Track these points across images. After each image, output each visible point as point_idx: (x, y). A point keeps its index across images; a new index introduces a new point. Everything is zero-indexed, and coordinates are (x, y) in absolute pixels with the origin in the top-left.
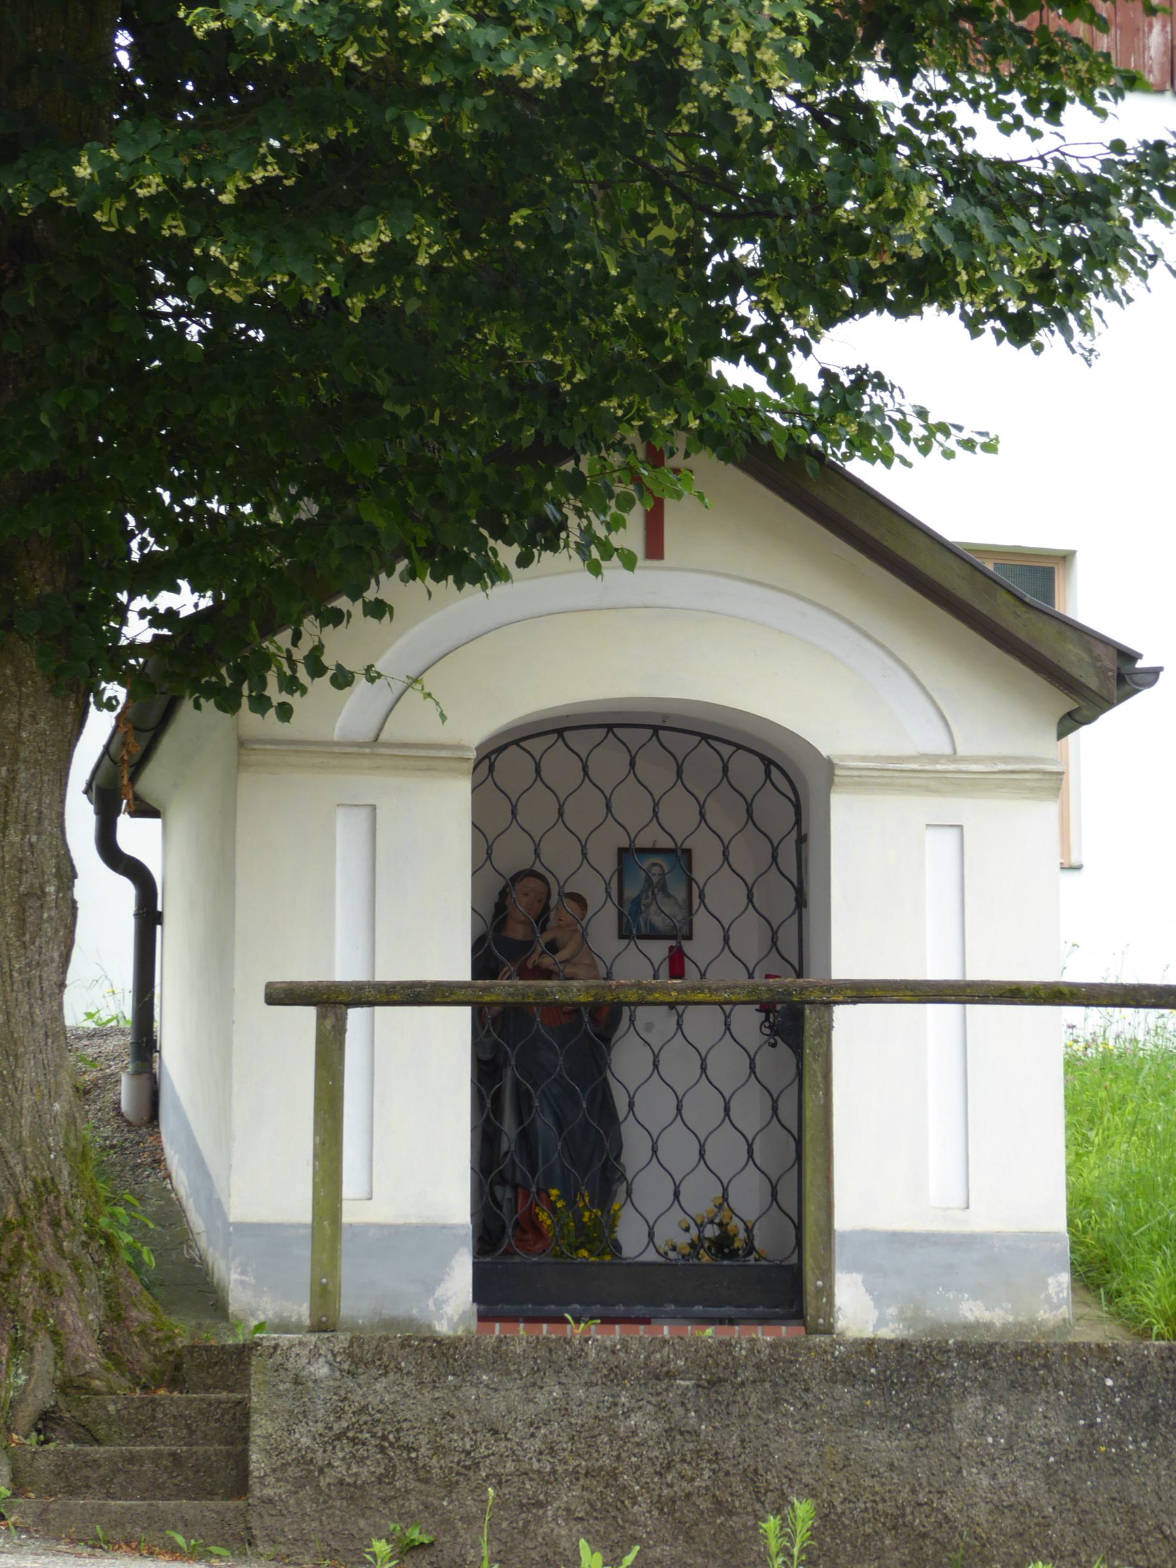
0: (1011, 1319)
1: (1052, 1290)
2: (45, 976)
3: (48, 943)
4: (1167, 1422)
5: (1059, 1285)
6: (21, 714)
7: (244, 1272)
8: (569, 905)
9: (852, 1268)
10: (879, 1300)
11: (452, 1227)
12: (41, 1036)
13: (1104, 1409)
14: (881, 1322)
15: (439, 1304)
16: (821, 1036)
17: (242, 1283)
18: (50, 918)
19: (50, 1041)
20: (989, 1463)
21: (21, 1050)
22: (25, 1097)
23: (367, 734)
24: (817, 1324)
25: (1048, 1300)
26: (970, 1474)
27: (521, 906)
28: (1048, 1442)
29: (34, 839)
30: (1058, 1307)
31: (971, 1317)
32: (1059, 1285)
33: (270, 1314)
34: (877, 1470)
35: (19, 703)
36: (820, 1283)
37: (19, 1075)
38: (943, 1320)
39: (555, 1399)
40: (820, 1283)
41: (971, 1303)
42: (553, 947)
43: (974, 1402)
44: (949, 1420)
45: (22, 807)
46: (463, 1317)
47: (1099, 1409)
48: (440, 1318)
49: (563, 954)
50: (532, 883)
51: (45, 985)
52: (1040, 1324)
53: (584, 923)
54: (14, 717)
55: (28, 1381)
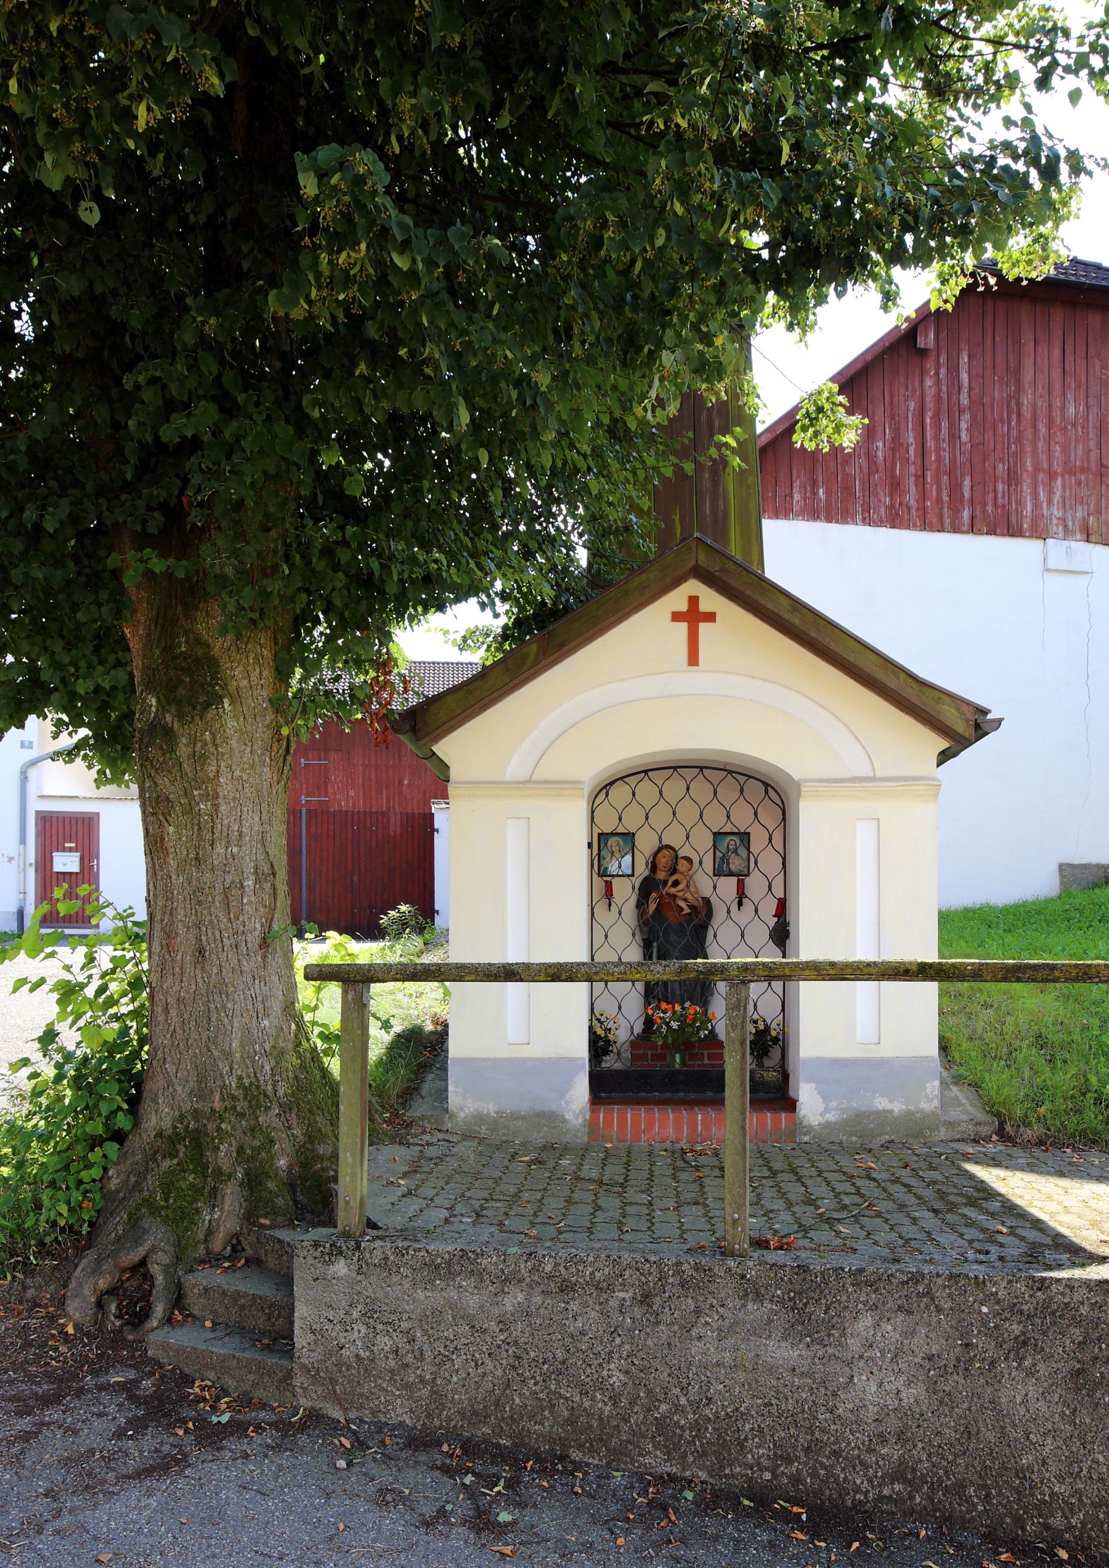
0: (904, 1107)
1: (928, 1091)
2: (249, 940)
3: (250, 918)
4: (1036, 1345)
5: (933, 1087)
6: (219, 766)
7: (456, 1086)
8: (685, 862)
9: (808, 1081)
10: (826, 1097)
11: (571, 1060)
12: (249, 980)
13: (980, 1332)
14: (827, 1110)
15: (568, 1103)
16: (739, 1010)
17: (456, 1092)
18: (250, 902)
19: (257, 982)
20: (876, 1372)
21: (231, 989)
22: (235, 1020)
23: (527, 778)
24: (733, 1248)
25: (927, 1095)
26: (860, 1380)
27: (663, 860)
28: (930, 1358)
29: (235, 850)
30: (932, 1100)
31: (880, 1107)
32: (933, 1087)
33: (472, 1109)
34: (781, 1373)
35: (217, 759)
36: (736, 1216)
37: (230, 1006)
38: (864, 1109)
39: (519, 1303)
40: (736, 1216)
41: (880, 1099)
42: (676, 884)
43: (866, 1321)
44: (843, 1334)
45: (225, 829)
46: (582, 1110)
47: (976, 1332)
48: (568, 1111)
49: (681, 887)
50: (665, 852)
51: (249, 945)
52: (922, 1111)
53: (691, 873)
54: (214, 768)
55: (221, 1216)
